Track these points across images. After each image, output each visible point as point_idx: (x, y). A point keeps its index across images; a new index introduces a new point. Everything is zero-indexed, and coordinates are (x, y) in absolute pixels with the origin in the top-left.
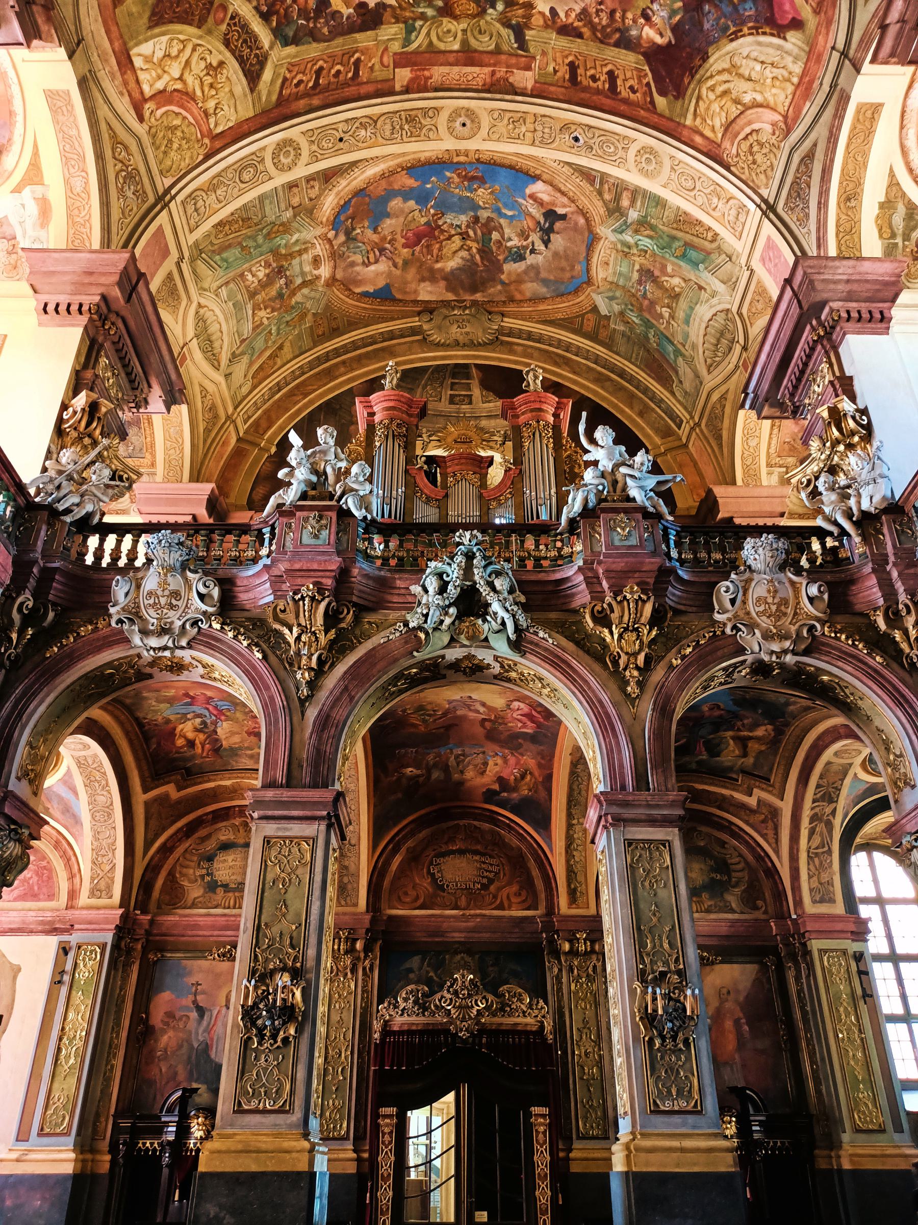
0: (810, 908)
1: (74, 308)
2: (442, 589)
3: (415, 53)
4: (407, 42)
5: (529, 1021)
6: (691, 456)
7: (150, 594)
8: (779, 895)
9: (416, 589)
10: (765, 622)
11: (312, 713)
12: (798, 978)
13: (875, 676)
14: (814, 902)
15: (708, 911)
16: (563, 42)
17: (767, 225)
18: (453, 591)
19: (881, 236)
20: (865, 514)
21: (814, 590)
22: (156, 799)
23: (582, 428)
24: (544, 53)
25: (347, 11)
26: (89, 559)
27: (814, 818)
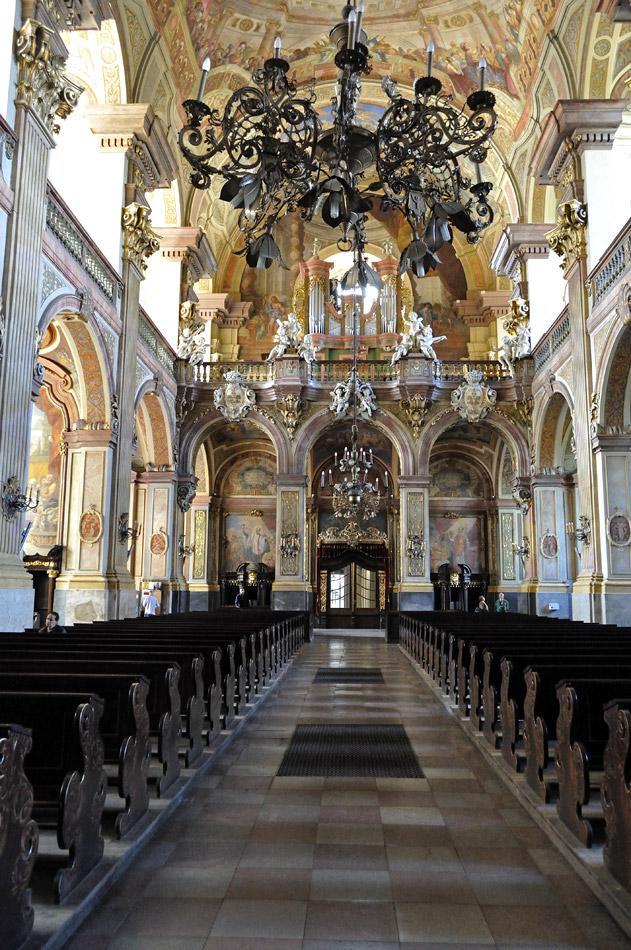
0: (501, 496)
1: (176, 254)
2: (343, 395)
3: (326, 64)
4: (321, 60)
5: (379, 541)
6: (477, 256)
7: (229, 397)
8: (490, 490)
9: (332, 393)
10: (470, 407)
11: (295, 446)
12: (492, 524)
13: (509, 428)
14: (503, 493)
15: (459, 496)
16: (406, 61)
17: (506, 175)
18: (346, 396)
19: (556, 197)
20: (517, 359)
21: (490, 394)
22: (218, 451)
23: (403, 312)
24: (396, 64)
25: (289, 55)
26: (202, 379)
27: (506, 460)
